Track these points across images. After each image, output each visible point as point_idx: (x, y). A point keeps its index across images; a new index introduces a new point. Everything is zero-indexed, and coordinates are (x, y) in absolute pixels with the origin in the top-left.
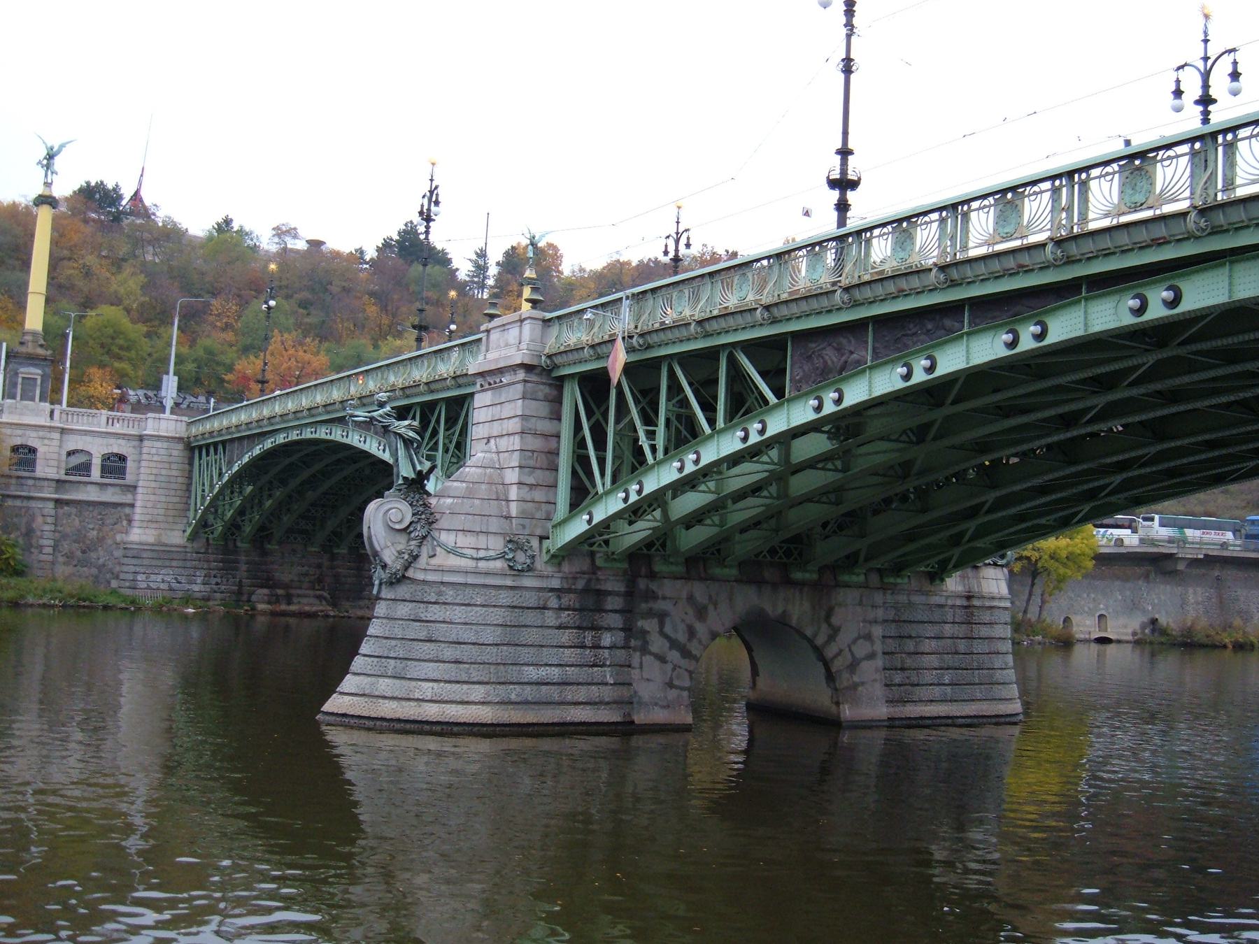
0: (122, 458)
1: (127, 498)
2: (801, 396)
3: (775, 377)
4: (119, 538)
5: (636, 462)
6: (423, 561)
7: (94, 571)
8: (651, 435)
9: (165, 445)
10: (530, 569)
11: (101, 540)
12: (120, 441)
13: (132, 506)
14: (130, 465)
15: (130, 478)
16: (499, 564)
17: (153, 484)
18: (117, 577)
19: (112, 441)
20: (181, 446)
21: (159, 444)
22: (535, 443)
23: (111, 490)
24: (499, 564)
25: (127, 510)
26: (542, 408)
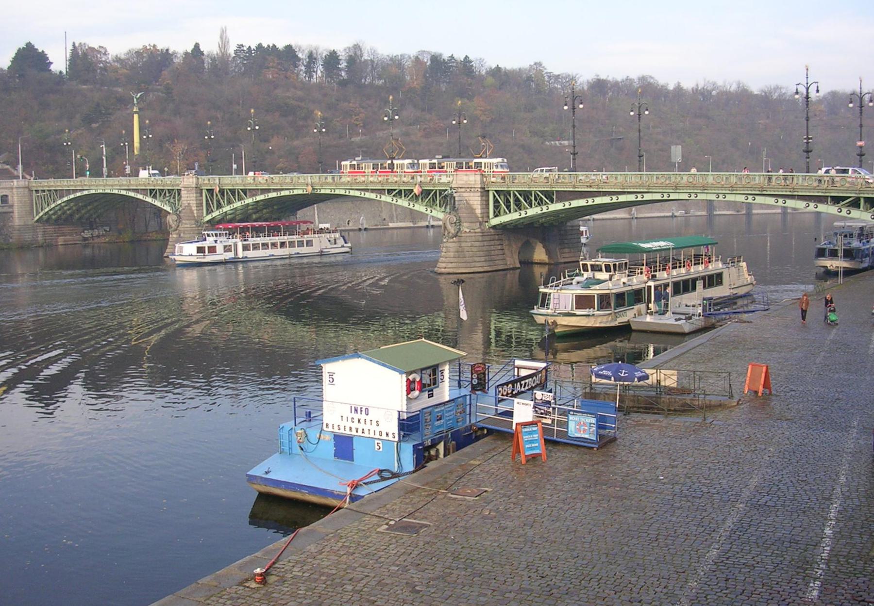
0: (7, 196)
1: (10, 210)
2: (250, 197)
3: (245, 194)
4: (10, 224)
5: (219, 206)
6: (180, 226)
7: (4, 237)
8: (224, 202)
9: (23, 190)
10: (200, 226)
11: (4, 225)
12: (6, 190)
13: (13, 212)
14: (9, 197)
15: (10, 202)
16: (194, 226)
17: (20, 204)
18: (11, 238)
19: (3, 190)
20: (27, 190)
21: (20, 190)
22: (198, 202)
23: (6, 208)
24: (194, 226)
25: (11, 214)
26: (199, 195)
